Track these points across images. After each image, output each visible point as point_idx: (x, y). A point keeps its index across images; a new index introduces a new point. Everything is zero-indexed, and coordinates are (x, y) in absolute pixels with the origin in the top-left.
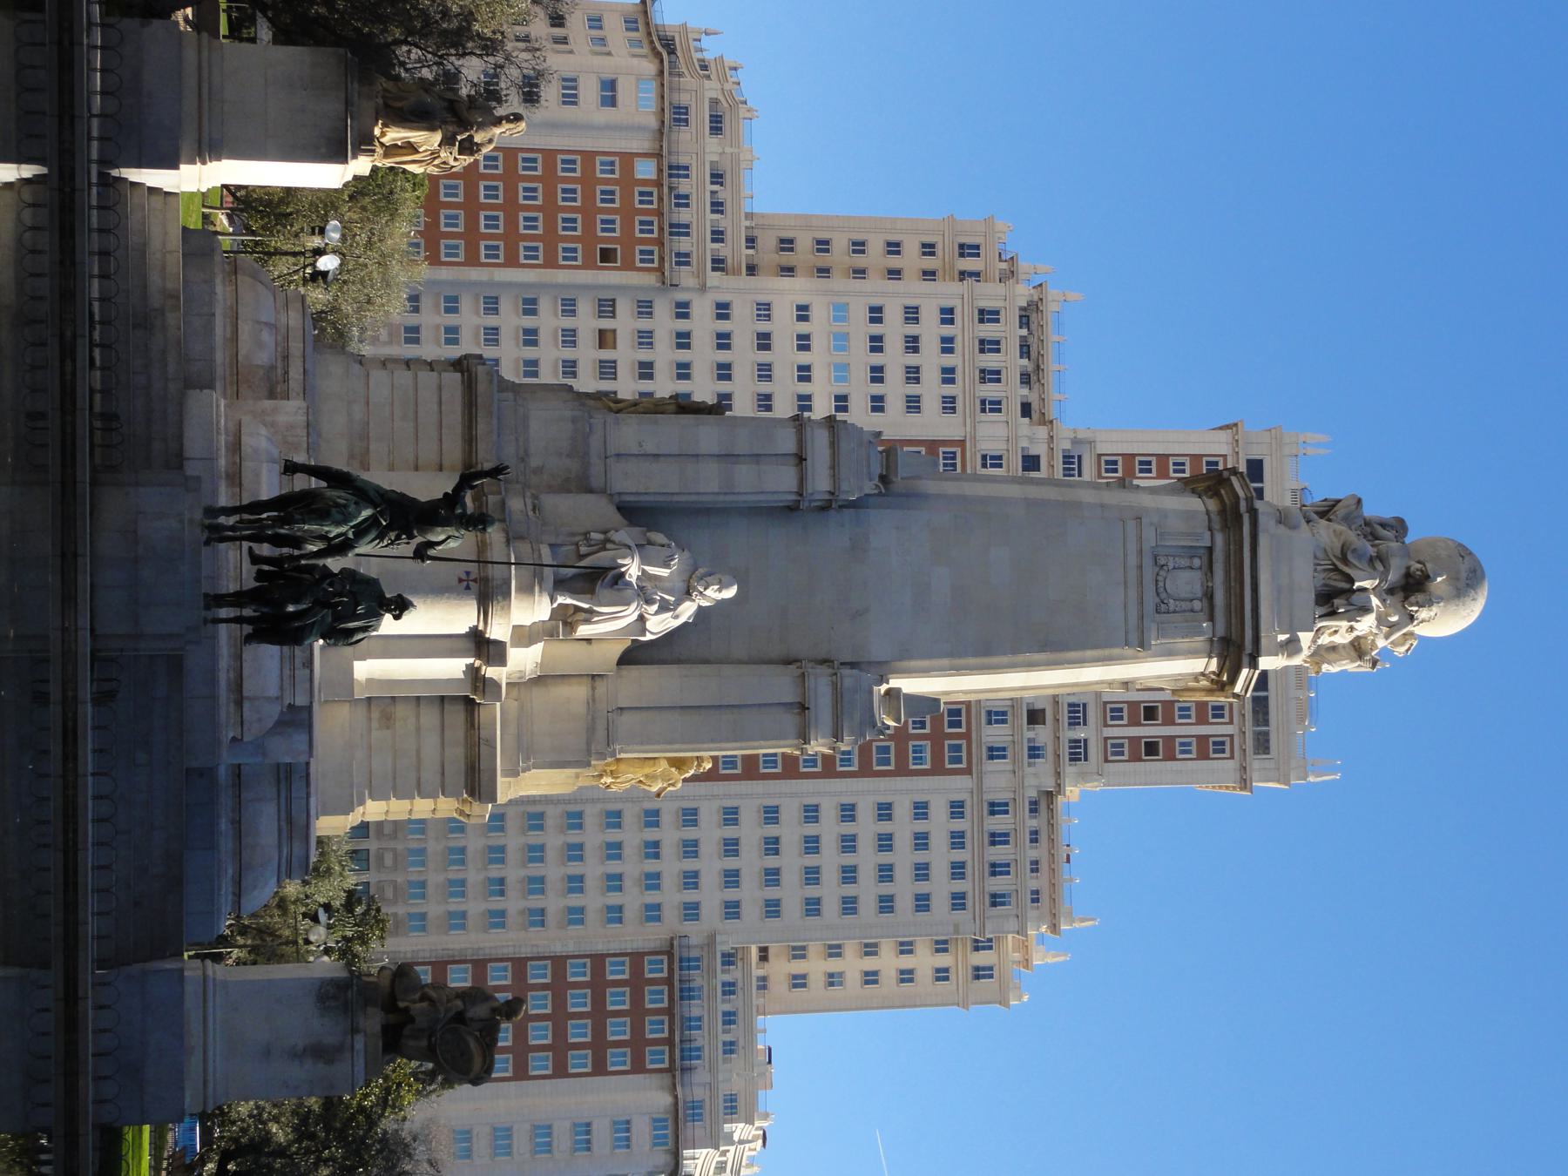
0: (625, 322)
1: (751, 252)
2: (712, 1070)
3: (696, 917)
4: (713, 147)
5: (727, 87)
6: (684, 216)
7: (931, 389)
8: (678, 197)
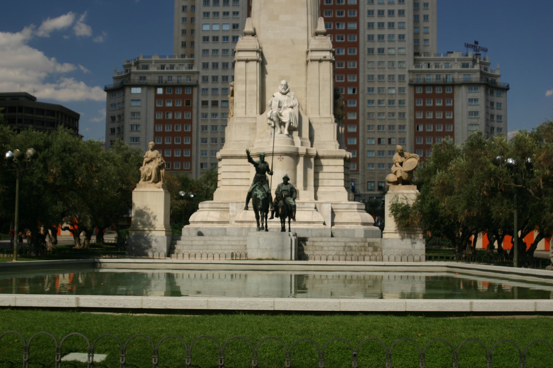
1: (186, 57)
2: (453, 72)
3: (404, 76)
4: (153, 69)
5: (133, 64)
8: (169, 80)
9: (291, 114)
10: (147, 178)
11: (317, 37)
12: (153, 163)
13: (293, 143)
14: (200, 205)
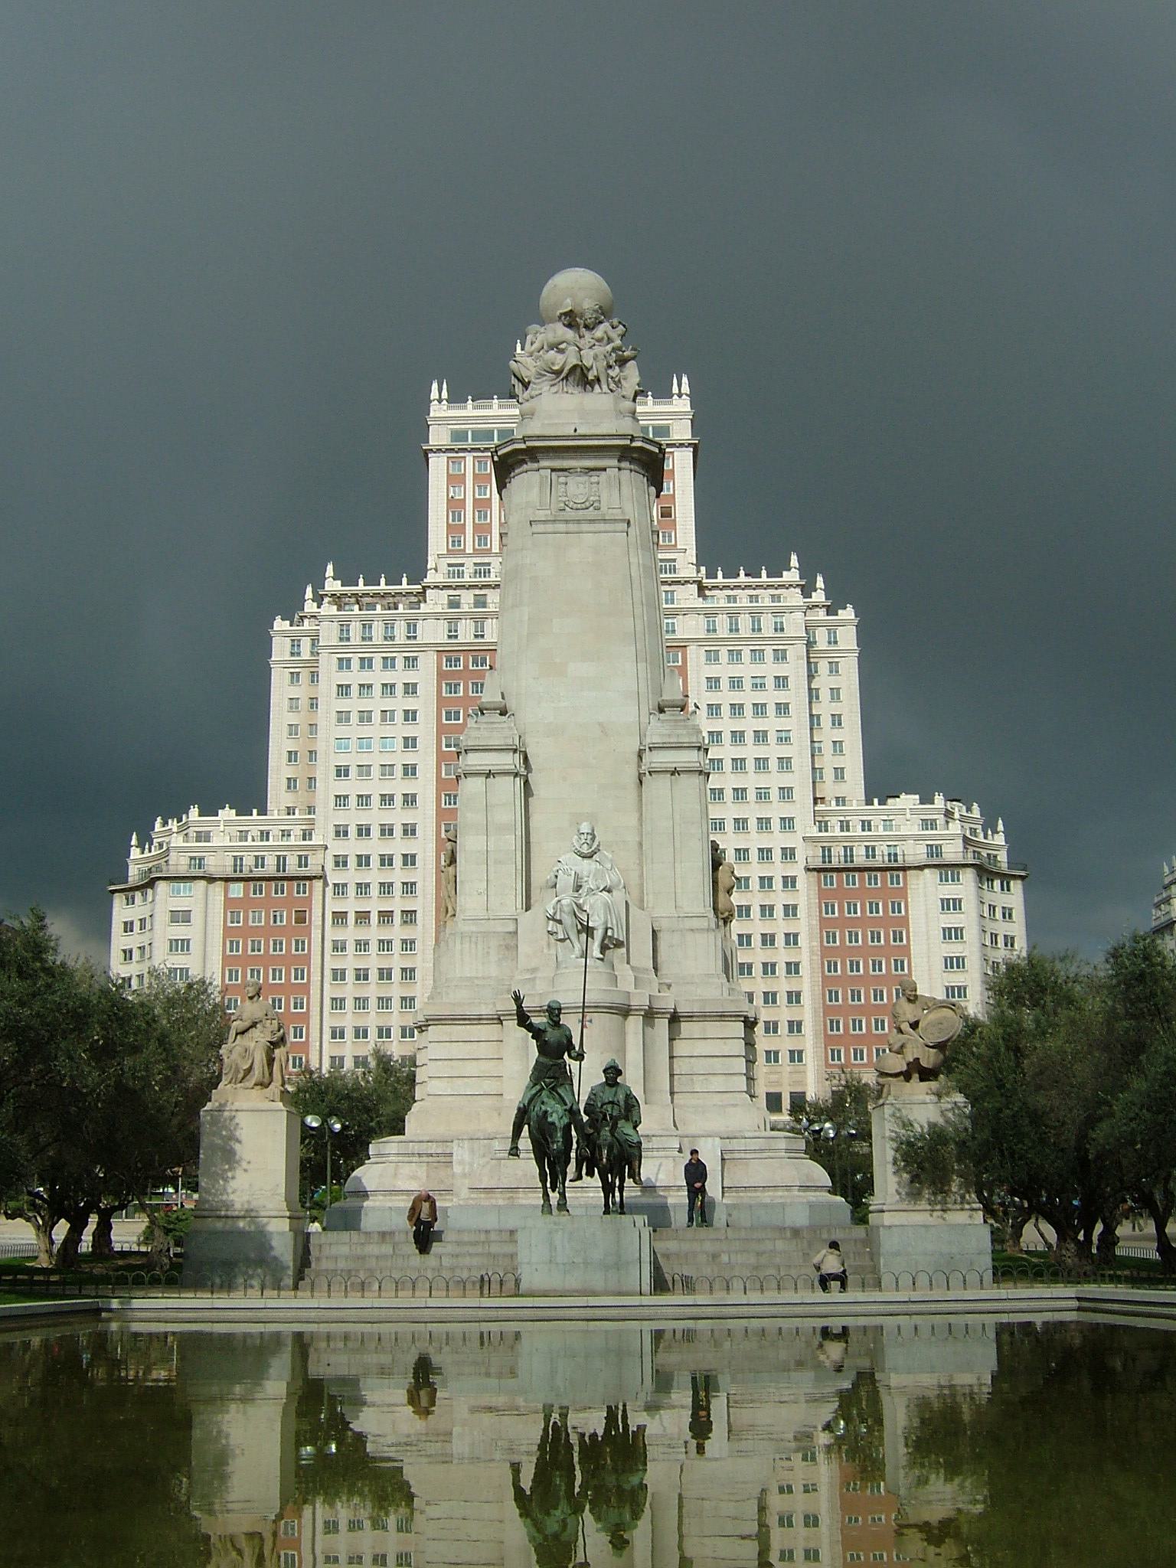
0: (351, 905)
2: (903, 838)
5: (175, 829)
6: (271, 862)
7: (399, 676)
9: (608, 907)
10: (240, 1076)
11: (662, 715)
12: (255, 1033)
13: (614, 979)
14: (372, 1149)
